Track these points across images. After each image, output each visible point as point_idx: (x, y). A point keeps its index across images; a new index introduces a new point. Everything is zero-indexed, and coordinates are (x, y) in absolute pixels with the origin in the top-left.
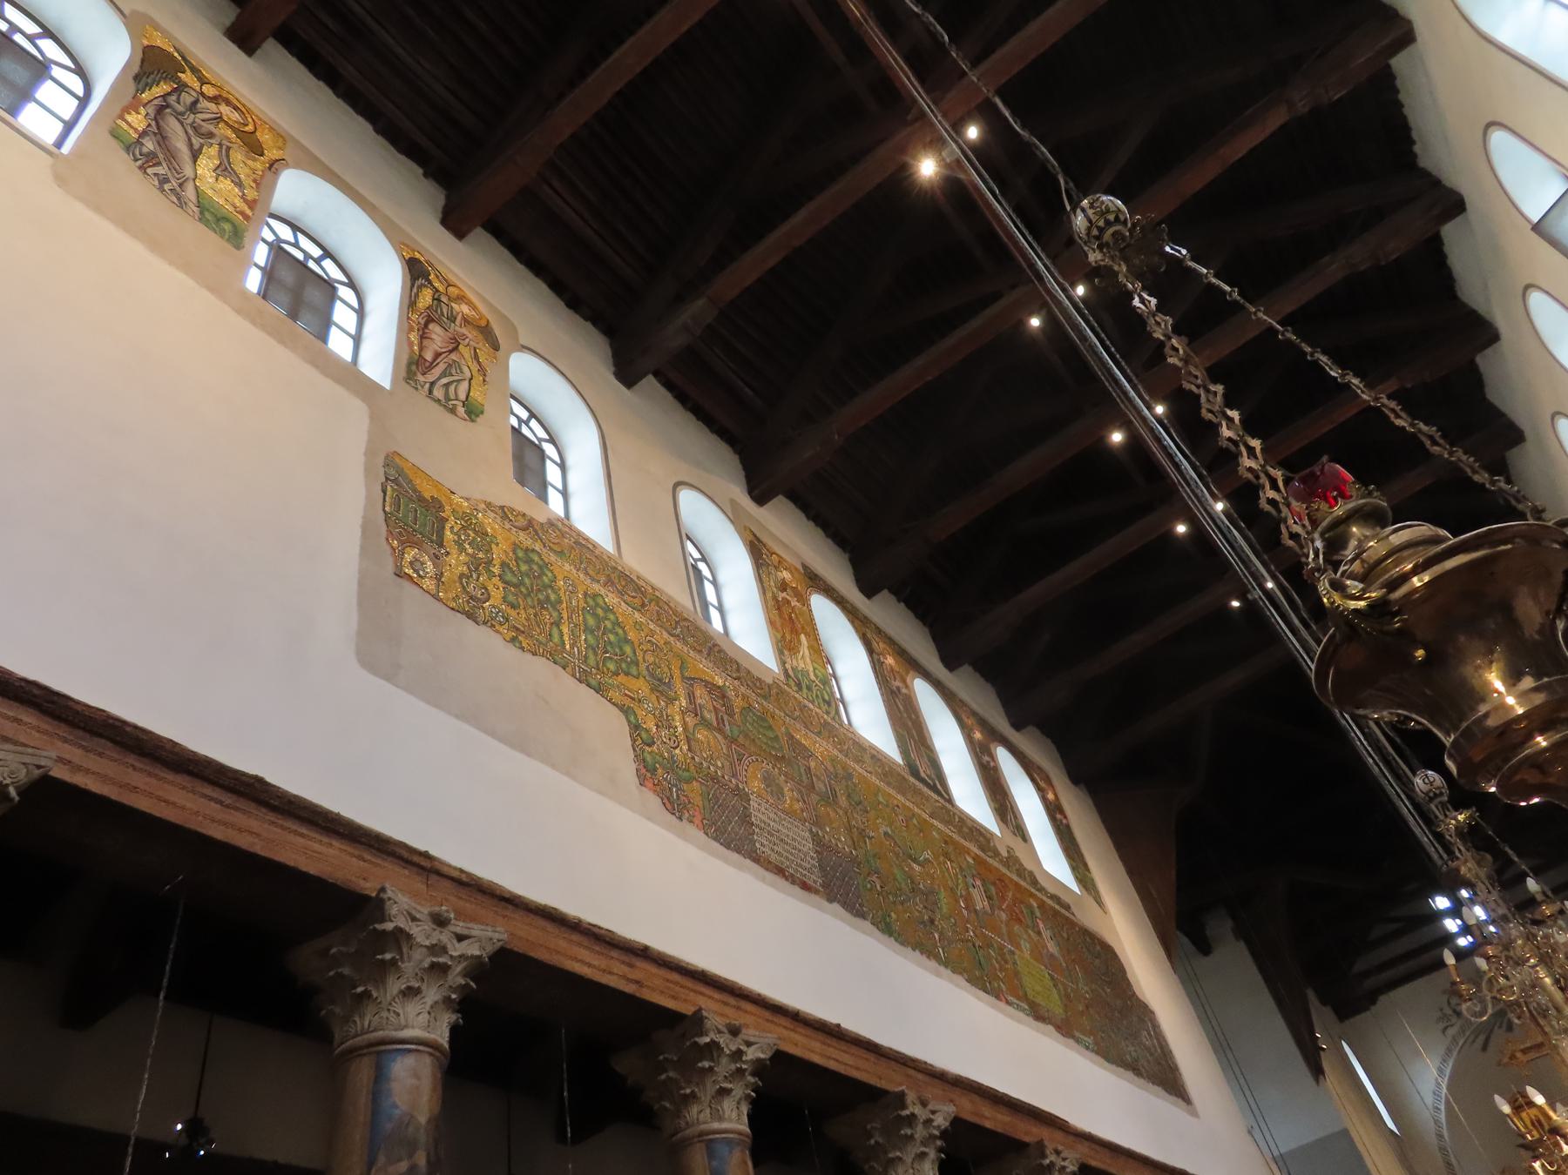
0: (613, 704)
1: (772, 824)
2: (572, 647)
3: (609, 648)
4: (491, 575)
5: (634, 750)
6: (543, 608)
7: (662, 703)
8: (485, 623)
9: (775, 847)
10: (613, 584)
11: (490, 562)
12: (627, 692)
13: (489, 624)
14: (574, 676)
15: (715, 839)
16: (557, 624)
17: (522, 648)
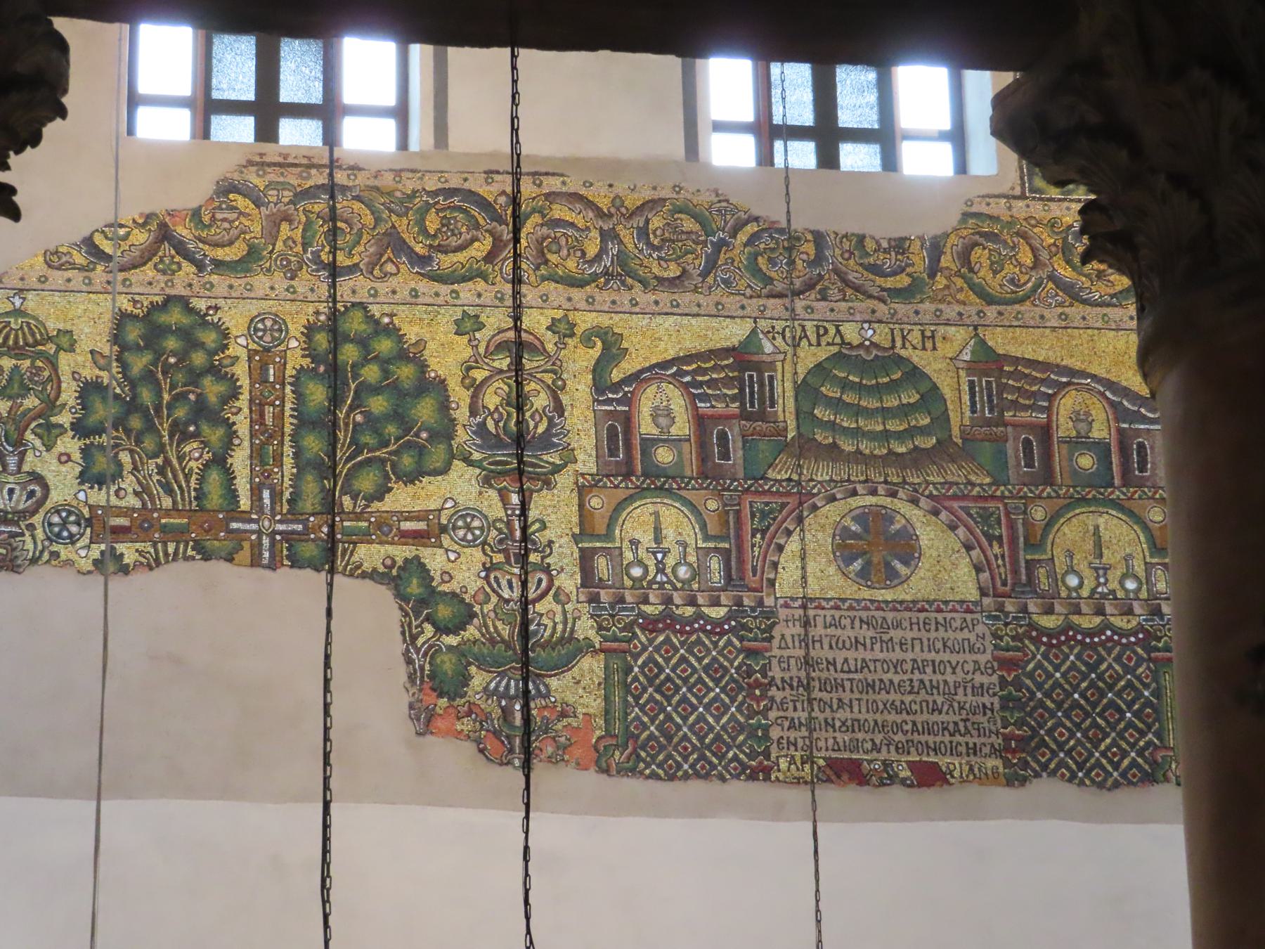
0: (364, 575)
1: (840, 656)
2: (256, 492)
3: (367, 439)
4: (50, 433)
5: (409, 662)
6: (186, 437)
8: (34, 561)
9: (841, 715)
10: (401, 247)
11: (51, 405)
12: (407, 526)
13: (46, 556)
14: (255, 562)
15: (633, 771)
16: (220, 461)
17: (125, 570)
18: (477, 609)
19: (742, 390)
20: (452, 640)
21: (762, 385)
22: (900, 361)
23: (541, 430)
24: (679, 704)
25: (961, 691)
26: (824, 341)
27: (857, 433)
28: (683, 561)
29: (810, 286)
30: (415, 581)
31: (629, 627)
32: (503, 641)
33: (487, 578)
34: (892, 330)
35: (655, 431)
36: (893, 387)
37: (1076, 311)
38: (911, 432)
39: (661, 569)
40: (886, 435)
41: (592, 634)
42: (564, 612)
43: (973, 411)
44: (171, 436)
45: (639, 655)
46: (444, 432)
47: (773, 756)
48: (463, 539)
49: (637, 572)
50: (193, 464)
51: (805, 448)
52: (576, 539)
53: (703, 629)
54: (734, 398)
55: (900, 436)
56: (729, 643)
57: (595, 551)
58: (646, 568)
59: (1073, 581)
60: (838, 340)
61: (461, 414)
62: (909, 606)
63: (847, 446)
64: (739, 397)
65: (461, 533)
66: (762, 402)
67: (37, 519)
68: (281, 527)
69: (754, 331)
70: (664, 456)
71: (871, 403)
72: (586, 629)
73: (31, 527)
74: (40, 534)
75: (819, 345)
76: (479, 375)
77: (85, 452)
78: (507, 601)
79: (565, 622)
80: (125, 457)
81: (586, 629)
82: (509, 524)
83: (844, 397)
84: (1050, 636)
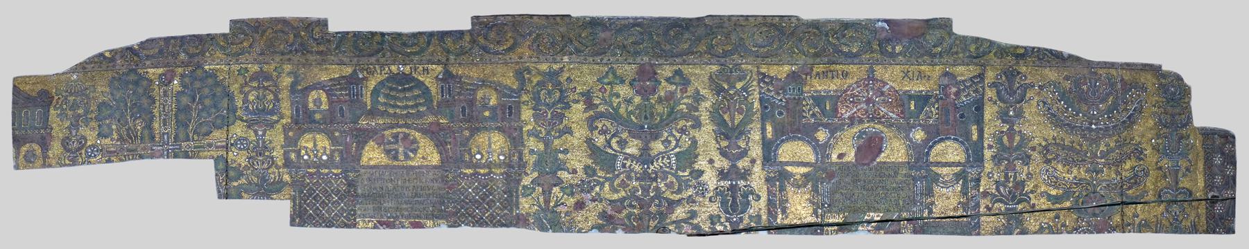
7: (260, 133)
18: (245, 172)
19: (350, 92)
20: (235, 184)
21: (358, 90)
22: (414, 79)
23: (271, 107)
24: (321, 203)
25: (431, 196)
26: (383, 72)
27: (395, 106)
28: (324, 153)
29: (378, 52)
30: (221, 163)
31: (303, 177)
32: (255, 183)
33: (249, 162)
34: (411, 68)
35: (315, 108)
36: (410, 89)
37: (487, 57)
38: (416, 106)
39: (316, 156)
40: (406, 107)
41: (288, 179)
42: (279, 173)
43: (443, 96)
44: (131, 118)
45: (306, 187)
46: (232, 109)
47: (357, 220)
48: (240, 148)
49: (306, 157)
50: (139, 128)
51: (372, 113)
52: (282, 147)
53: (331, 177)
54: (346, 95)
55: (412, 107)
56: (342, 181)
57: (289, 152)
58: (310, 157)
59: (478, 157)
60: (389, 72)
61: (239, 103)
62: (413, 168)
63: (391, 111)
64: (349, 95)
65: (239, 146)
66: (357, 95)
67: (83, 151)
68: (170, 147)
69: (355, 70)
70: (318, 116)
71: (401, 95)
72: (287, 178)
73: (81, 154)
74: (84, 156)
75: (381, 74)
76: (247, 89)
77: (99, 126)
78: (256, 169)
79: (279, 176)
80: (114, 127)
81: (287, 178)
82: (258, 143)
83: (391, 93)
84: (468, 177)
